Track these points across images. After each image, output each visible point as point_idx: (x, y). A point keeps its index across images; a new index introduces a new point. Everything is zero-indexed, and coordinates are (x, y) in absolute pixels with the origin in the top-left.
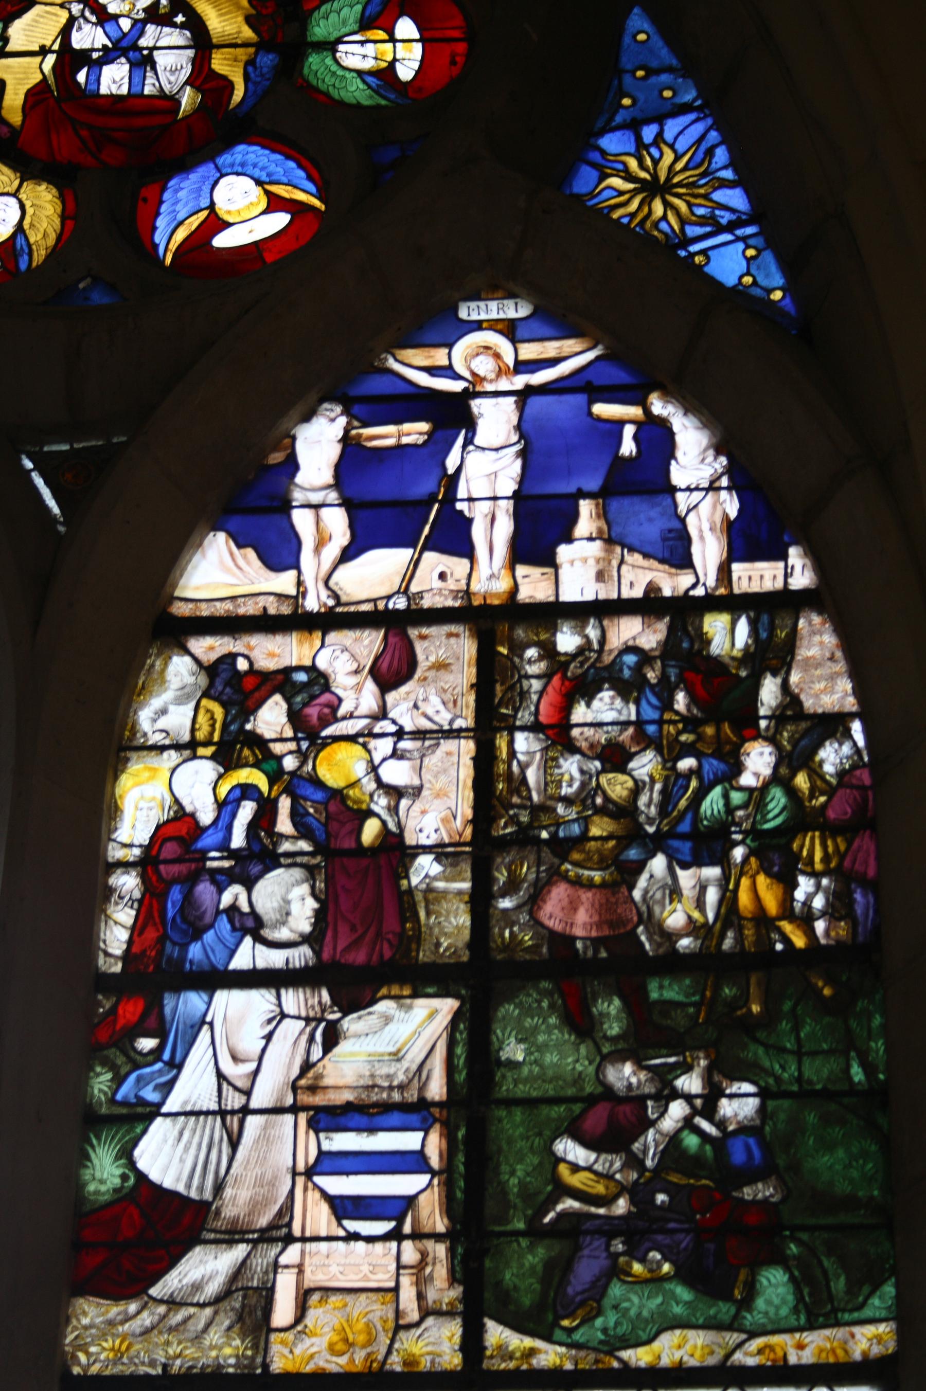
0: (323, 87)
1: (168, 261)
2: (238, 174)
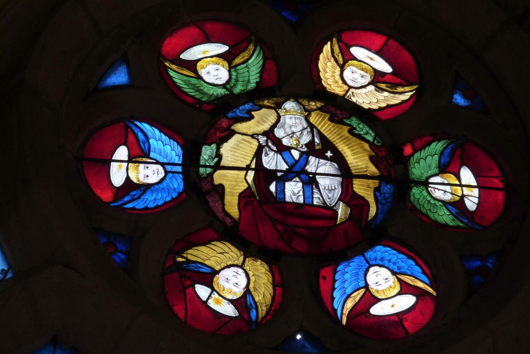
0: (424, 210)
2: (380, 266)
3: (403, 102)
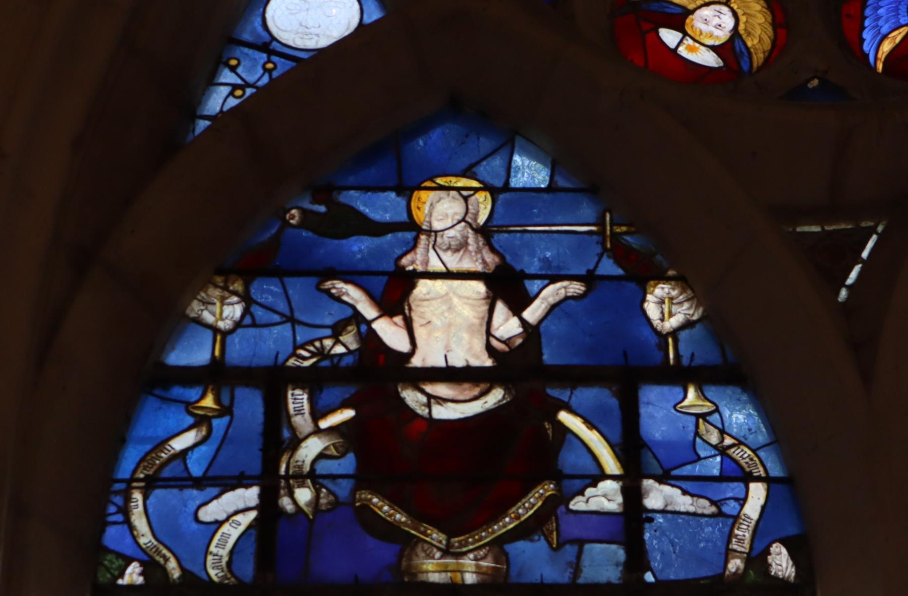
1: (880, 66)
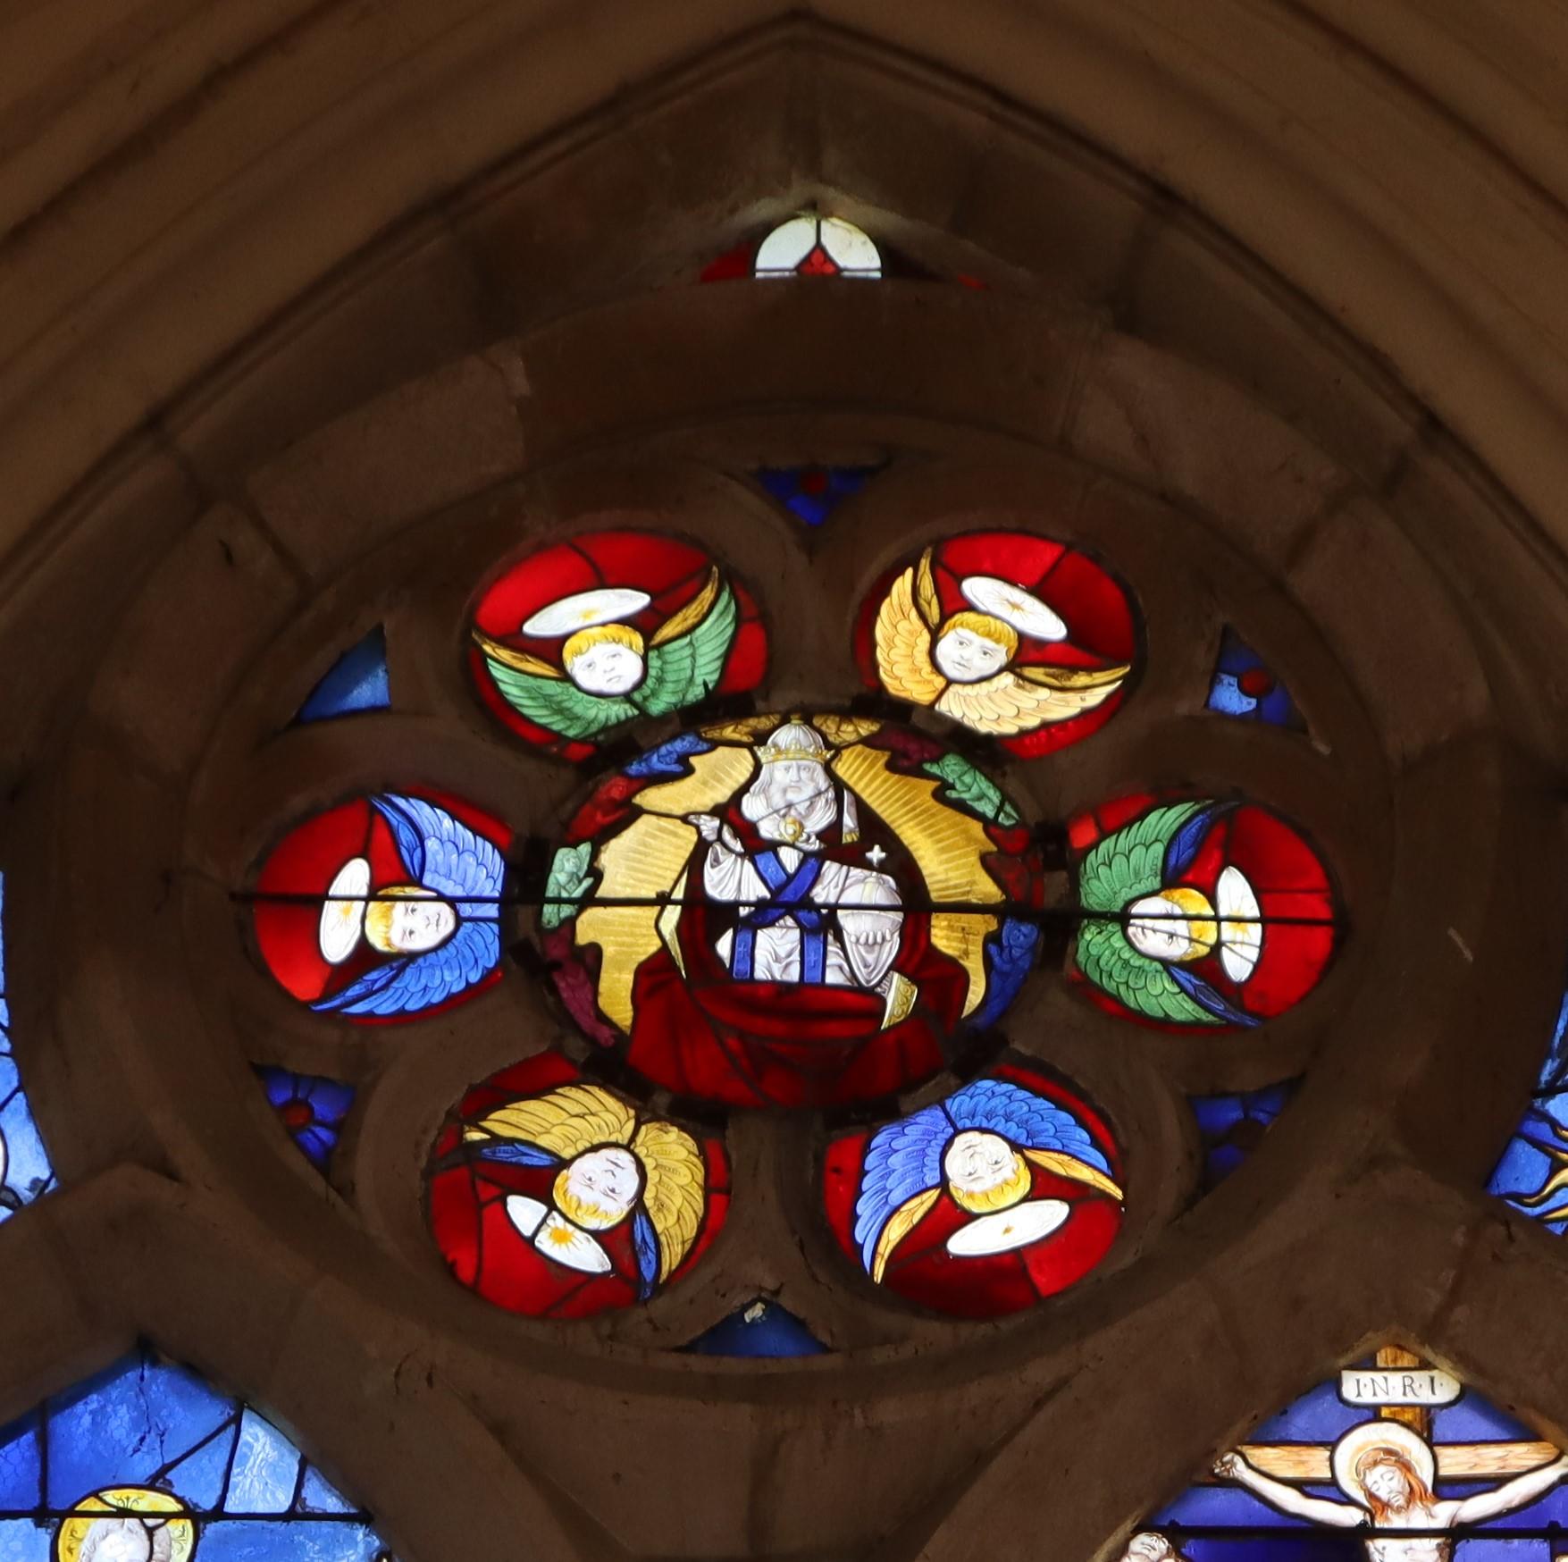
0: (1109, 986)
2: (983, 1131)
3: (1086, 714)
